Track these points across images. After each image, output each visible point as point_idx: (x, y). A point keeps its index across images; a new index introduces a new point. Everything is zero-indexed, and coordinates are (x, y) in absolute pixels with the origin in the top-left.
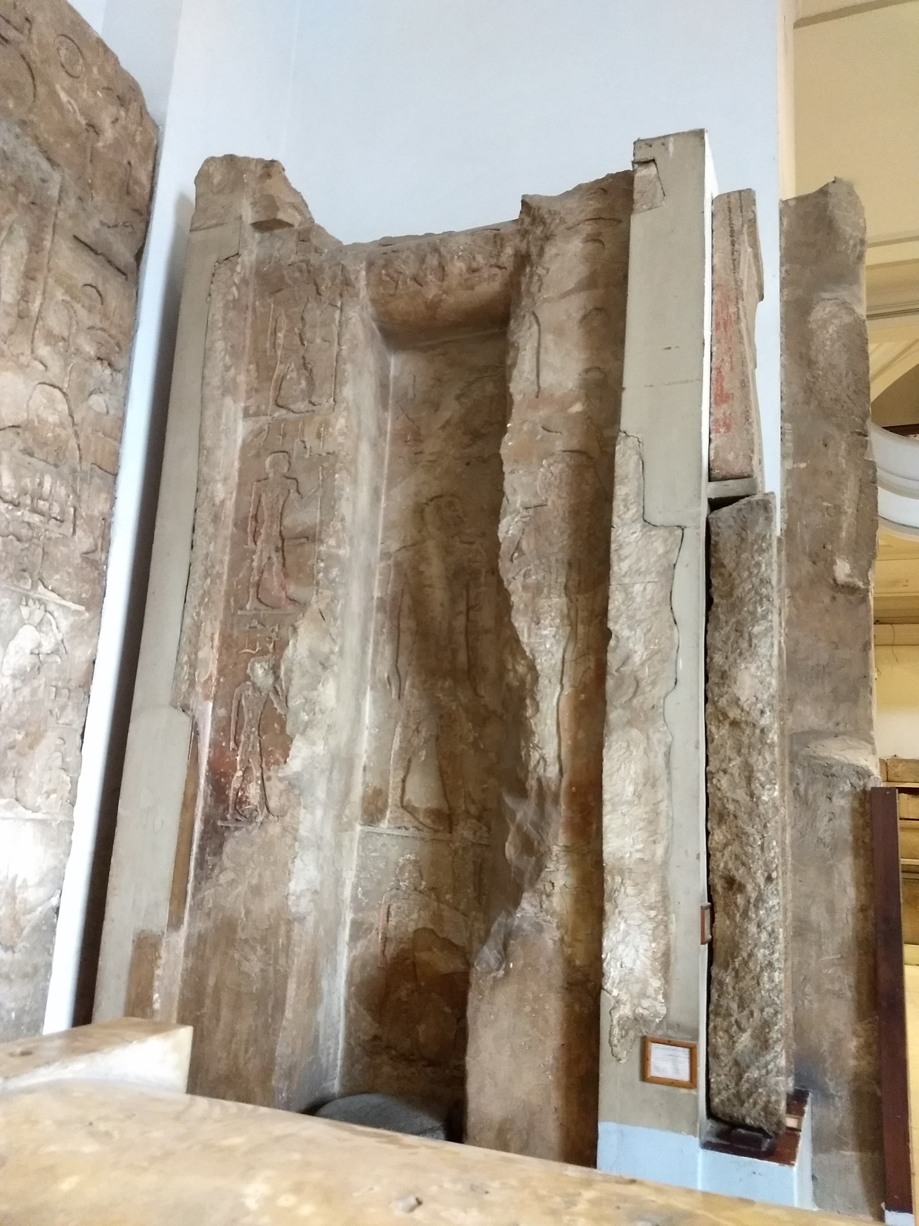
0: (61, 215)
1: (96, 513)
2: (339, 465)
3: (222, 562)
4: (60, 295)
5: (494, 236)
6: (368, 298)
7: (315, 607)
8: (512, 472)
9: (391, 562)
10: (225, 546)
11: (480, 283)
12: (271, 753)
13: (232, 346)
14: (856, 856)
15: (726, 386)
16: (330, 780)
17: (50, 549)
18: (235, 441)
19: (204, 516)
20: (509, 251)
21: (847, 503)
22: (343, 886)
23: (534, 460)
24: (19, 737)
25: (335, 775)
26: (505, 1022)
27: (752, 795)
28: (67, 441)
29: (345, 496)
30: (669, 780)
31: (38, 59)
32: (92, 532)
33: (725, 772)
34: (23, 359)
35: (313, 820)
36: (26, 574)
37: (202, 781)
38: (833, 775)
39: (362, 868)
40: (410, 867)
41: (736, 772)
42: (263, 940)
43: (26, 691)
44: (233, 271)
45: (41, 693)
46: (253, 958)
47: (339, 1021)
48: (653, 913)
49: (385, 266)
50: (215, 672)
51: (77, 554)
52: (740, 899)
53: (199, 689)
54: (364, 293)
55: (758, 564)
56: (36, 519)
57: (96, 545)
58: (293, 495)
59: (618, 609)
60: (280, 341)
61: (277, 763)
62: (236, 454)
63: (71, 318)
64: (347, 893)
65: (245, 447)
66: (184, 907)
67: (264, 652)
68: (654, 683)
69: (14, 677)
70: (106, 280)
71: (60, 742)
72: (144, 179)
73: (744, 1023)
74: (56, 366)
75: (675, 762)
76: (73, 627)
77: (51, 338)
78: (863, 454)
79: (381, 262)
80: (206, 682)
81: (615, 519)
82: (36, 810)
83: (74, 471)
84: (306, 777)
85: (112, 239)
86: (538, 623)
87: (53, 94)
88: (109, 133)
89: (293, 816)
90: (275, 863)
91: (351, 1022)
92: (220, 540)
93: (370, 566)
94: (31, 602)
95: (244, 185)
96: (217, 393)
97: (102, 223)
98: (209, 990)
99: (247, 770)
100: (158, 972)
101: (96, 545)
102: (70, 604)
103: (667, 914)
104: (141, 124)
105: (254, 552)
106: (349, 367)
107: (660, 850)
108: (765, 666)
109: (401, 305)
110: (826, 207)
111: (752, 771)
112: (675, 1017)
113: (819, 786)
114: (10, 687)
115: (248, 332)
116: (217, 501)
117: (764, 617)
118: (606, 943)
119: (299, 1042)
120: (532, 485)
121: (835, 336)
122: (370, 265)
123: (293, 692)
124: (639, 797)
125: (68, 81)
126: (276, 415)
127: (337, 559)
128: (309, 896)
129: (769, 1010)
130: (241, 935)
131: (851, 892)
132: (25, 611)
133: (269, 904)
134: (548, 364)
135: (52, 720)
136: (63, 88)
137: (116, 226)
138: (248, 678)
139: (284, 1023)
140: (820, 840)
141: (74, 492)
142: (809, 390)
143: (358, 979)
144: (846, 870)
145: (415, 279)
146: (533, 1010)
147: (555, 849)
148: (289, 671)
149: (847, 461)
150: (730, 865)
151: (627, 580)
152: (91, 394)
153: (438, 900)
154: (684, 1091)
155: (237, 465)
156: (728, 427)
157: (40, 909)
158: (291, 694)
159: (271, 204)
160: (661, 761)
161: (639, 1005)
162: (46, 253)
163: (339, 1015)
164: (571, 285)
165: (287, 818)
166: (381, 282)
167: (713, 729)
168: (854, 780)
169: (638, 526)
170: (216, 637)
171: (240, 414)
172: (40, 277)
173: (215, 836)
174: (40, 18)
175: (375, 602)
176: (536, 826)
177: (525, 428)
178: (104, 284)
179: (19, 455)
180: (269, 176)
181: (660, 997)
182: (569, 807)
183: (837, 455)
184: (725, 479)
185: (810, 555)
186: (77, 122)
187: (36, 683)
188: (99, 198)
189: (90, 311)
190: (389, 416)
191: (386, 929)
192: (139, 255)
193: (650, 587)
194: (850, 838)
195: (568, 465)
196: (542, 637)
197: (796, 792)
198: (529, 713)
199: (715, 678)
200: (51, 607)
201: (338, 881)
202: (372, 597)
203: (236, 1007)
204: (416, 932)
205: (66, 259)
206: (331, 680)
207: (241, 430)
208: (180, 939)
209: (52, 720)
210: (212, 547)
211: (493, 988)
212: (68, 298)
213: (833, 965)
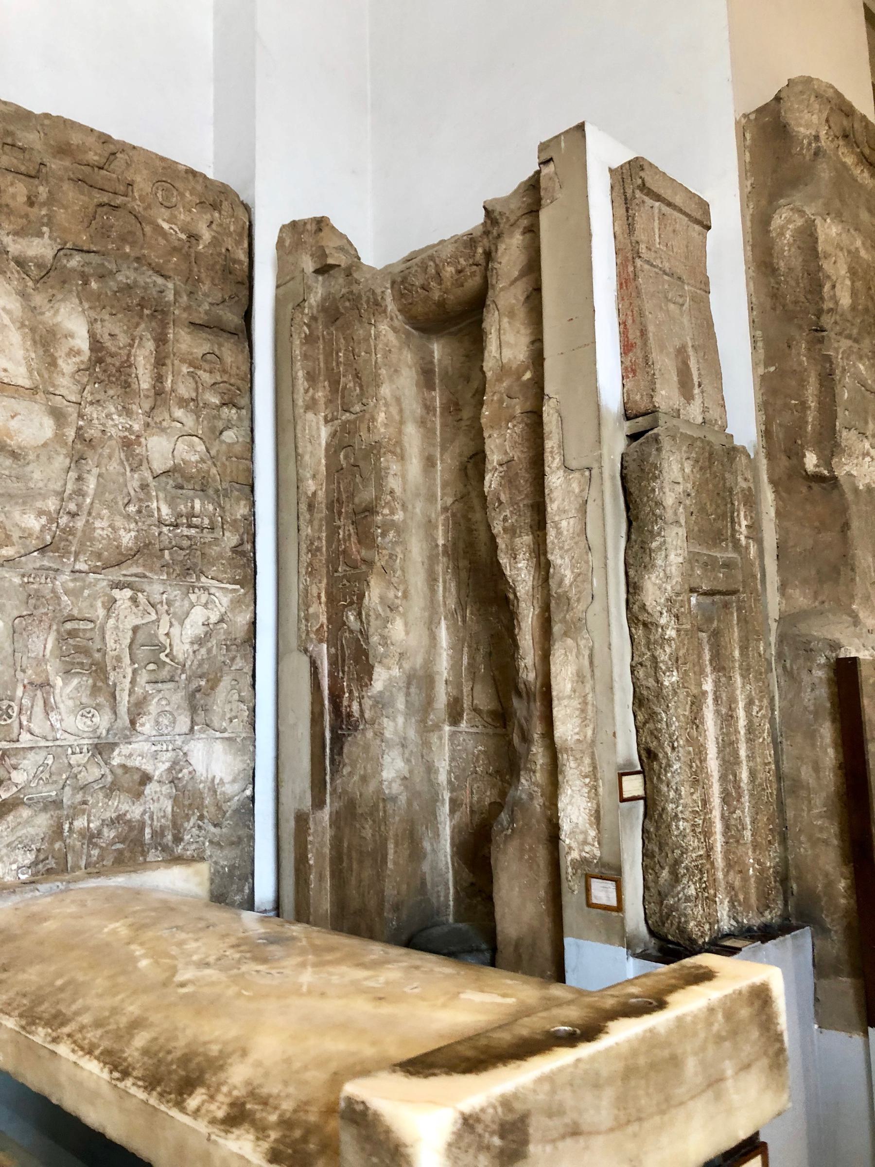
0: (177, 312)
1: (239, 517)
2: (383, 450)
3: (319, 538)
4: (185, 369)
5: (470, 241)
6: (395, 309)
7: (378, 564)
8: (490, 437)
9: (449, 514)
10: (321, 526)
11: (466, 280)
12: (362, 678)
13: (308, 373)
14: (834, 721)
15: (631, 337)
16: (408, 694)
17: (207, 550)
18: (320, 444)
19: (304, 507)
20: (480, 250)
21: (810, 398)
22: (437, 772)
23: (503, 424)
24: (203, 683)
25: (413, 690)
26: (514, 867)
27: (657, 681)
28: (208, 472)
29: (392, 472)
30: (593, 676)
31: (141, 209)
32: (237, 531)
33: (641, 664)
34: (165, 424)
35: (396, 725)
36: (191, 572)
37: (326, 702)
38: (811, 650)
39: (452, 759)
40: (482, 756)
41: (648, 664)
42: (371, 814)
43: (203, 651)
44: (303, 313)
45: (214, 651)
46: (367, 826)
47: (447, 872)
48: (587, 780)
49: (402, 282)
50: (325, 621)
51: (228, 549)
52: (655, 765)
53: (313, 636)
54: (391, 306)
55: (653, 490)
56: (193, 531)
57: (242, 540)
58: (358, 479)
59: (553, 543)
60: (341, 359)
61: (366, 685)
62: (322, 453)
63: (196, 383)
64: (443, 778)
65: (328, 445)
66: (325, 793)
67: (352, 603)
68: (578, 600)
69: (192, 643)
70: (220, 345)
71: (234, 683)
72: (242, 256)
73: (662, 861)
74: (189, 421)
75: (596, 662)
76: (232, 601)
77: (183, 403)
78: (820, 350)
79: (399, 279)
80: (318, 630)
81: (547, 469)
82: (224, 731)
83: (217, 491)
84: (387, 694)
85: (221, 313)
86: (515, 558)
87: (158, 229)
88: (207, 235)
89: (379, 724)
90: (372, 759)
91: (456, 873)
92: (316, 523)
93: (430, 521)
94: (196, 590)
95: (308, 236)
96: (302, 411)
97: (211, 304)
98: (345, 850)
99: (351, 692)
100: (310, 838)
101: (242, 540)
102: (228, 586)
103: (596, 780)
104: (233, 216)
105: (339, 527)
106: (383, 371)
107: (589, 732)
108: (662, 575)
109: (420, 309)
110: (779, 112)
111: (657, 663)
112: (606, 859)
113: (801, 661)
114: (191, 651)
115: (321, 357)
116: (310, 493)
117: (659, 534)
118: (560, 805)
119: (404, 887)
120: (501, 446)
121: (791, 241)
122: (393, 283)
123: (372, 630)
124: (575, 691)
125: (166, 213)
126: (344, 418)
127: (393, 524)
128: (399, 781)
129: (678, 852)
130: (359, 811)
131: (831, 751)
132: (193, 597)
133: (372, 787)
134: (505, 343)
135: (226, 668)
136: (164, 220)
137: (224, 301)
138: (344, 624)
139: (389, 872)
140: (806, 708)
141: (220, 506)
142: (775, 295)
143: (457, 841)
144: (827, 732)
145: (423, 288)
146: (530, 858)
147: (536, 736)
148: (368, 615)
149: (808, 359)
150: (649, 740)
151: (557, 519)
152: (221, 433)
153: (502, 780)
154: (614, 914)
155: (323, 461)
156: (634, 371)
157: (236, 798)
158: (370, 633)
159: (321, 253)
160: (586, 662)
161: (583, 850)
162: (170, 343)
163: (447, 868)
164: (516, 274)
165: (376, 726)
166: (402, 295)
167: (633, 630)
168: (828, 653)
169: (561, 473)
170: (323, 595)
171: (322, 422)
172: (168, 362)
173: (338, 741)
174: (138, 179)
175: (440, 549)
176: (527, 720)
177: (495, 398)
178: (219, 349)
179: (174, 491)
180: (320, 230)
181: (596, 844)
182: (542, 704)
183: (799, 354)
184: (636, 416)
185: (785, 451)
186: (179, 240)
187: (210, 645)
188: (205, 287)
189: (211, 372)
190: (437, 394)
191: (471, 803)
192: (248, 316)
193: (572, 521)
194: (828, 705)
195: (527, 425)
196: (519, 569)
197: (784, 667)
198: (517, 631)
199: (633, 588)
200: (212, 591)
201: (430, 769)
202: (437, 546)
203: (361, 862)
204: (491, 804)
205: (186, 343)
206: (398, 618)
207: (324, 433)
208: (325, 815)
209: (226, 668)
210: (309, 530)
211: (505, 842)
212: (192, 369)
213: (821, 817)
